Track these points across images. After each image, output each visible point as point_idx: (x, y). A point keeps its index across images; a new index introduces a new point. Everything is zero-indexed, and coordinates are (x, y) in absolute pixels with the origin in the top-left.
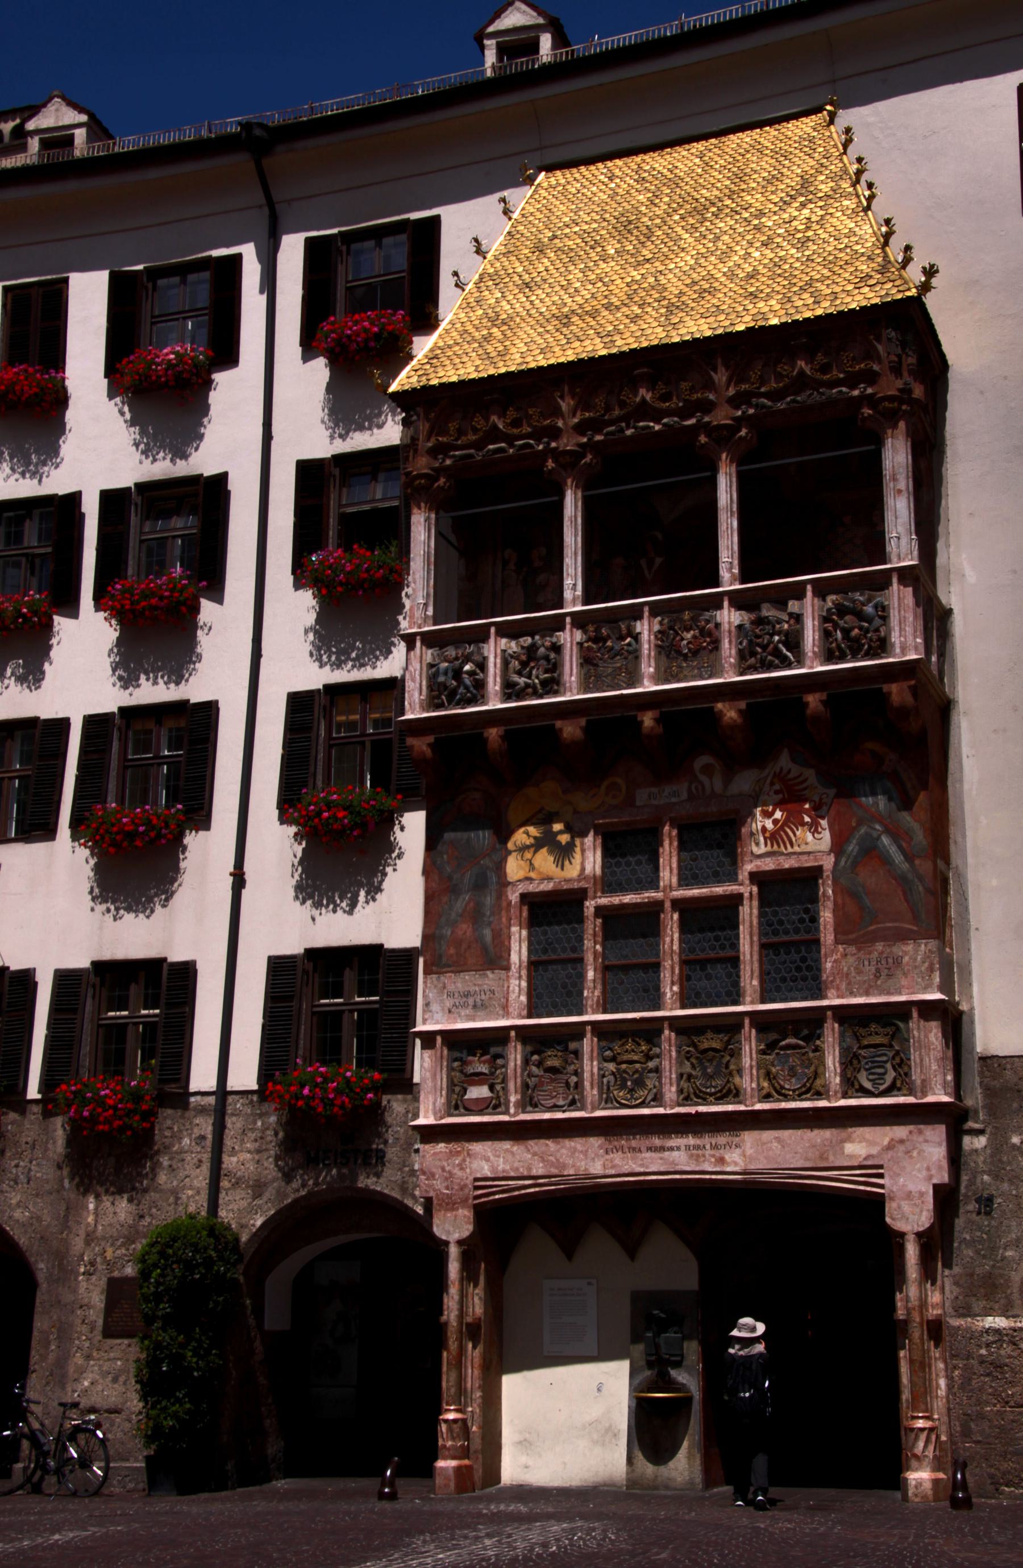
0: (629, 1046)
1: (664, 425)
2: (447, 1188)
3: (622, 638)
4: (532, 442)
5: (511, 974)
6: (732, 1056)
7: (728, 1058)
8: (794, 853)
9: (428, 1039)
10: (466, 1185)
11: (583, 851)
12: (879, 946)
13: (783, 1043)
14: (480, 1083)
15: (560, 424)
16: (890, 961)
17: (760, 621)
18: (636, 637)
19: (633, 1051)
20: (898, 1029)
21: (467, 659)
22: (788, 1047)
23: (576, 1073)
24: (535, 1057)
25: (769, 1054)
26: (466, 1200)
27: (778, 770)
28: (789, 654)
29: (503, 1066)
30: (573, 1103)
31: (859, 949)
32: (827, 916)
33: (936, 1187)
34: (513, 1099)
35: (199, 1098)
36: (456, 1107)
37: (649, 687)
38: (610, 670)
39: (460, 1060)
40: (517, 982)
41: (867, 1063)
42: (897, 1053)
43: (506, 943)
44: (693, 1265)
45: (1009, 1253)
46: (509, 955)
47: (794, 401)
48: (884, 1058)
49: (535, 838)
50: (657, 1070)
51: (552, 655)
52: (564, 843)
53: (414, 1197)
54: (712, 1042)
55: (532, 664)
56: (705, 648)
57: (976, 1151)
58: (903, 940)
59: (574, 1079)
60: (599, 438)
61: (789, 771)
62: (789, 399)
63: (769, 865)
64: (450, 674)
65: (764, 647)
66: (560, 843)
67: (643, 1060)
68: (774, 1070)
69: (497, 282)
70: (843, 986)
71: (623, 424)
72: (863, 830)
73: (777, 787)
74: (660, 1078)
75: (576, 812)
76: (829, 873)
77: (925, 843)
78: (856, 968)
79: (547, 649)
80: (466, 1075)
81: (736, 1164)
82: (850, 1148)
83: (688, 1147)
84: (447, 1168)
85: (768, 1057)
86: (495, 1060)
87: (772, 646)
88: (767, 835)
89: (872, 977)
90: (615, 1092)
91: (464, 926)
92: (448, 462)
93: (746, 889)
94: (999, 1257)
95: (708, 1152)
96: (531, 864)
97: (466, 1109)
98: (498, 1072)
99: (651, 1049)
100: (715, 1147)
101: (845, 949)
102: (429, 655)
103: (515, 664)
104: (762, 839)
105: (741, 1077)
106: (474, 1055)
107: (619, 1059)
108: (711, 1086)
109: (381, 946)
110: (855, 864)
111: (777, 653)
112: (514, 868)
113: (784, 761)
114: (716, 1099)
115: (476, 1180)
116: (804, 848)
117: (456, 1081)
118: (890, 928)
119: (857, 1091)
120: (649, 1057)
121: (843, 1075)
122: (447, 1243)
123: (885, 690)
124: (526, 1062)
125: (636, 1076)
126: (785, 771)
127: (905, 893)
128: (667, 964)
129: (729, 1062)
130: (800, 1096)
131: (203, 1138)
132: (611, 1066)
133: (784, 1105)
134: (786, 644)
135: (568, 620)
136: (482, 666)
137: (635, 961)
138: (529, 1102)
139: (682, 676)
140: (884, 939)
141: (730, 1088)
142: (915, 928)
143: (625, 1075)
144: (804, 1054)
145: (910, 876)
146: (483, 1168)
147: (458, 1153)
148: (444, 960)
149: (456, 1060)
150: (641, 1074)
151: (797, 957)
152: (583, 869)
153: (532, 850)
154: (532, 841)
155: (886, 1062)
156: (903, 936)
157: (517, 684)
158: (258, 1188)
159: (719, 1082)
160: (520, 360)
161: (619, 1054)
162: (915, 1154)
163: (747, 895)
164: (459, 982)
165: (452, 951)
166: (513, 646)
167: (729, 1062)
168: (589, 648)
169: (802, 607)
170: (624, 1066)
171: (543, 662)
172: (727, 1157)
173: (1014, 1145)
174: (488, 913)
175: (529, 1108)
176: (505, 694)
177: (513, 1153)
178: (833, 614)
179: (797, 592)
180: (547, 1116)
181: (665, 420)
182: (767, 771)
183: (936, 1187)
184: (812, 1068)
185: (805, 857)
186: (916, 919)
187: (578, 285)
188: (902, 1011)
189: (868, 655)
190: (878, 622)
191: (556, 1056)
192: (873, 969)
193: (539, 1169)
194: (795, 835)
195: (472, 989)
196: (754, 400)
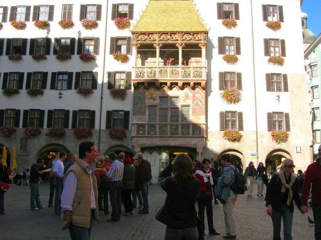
12: (198, 116)
14: (142, 131)
15: (157, 39)
23: (155, 130)
34: (146, 133)
35: (96, 130)
60: (163, 42)
72: (196, 100)
82: (193, 142)
100: (175, 141)
103: (149, 74)
104: (182, 100)
112: (147, 101)
113: (187, 90)
121: (192, 132)
124: (148, 128)
128: (169, 116)
130: (186, 135)
131: (97, 136)
133: (184, 136)
138: (149, 134)
145: (202, 107)
147: (138, 140)
156: (201, 115)
158: (106, 143)
164: (138, 116)
166: (150, 70)
180: (151, 136)
190: (201, 74)
193: (150, 143)
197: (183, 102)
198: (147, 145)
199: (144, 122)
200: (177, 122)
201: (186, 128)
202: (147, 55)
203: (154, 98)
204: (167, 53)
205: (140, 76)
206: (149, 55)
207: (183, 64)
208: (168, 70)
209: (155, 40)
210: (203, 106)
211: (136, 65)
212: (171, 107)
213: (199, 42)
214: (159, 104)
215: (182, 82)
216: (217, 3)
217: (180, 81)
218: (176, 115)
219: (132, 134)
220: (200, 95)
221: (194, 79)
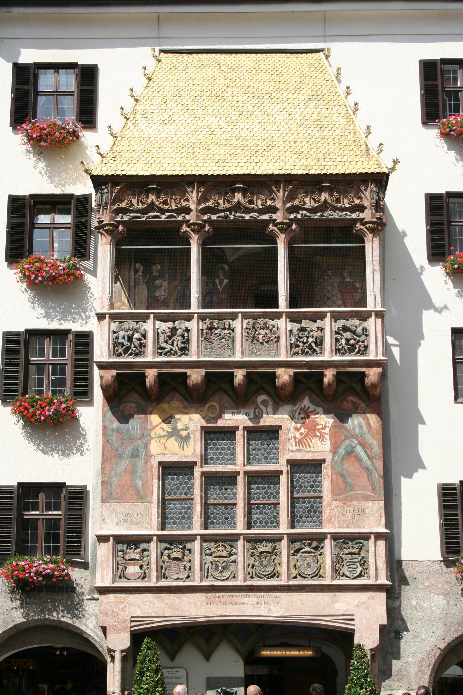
0: (220, 548)
1: (251, 217)
2: (116, 622)
3: (225, 329)
4: (175, 215)
5: (153, 505)
6: (276, 556)
7: (274, 557)
8: (311, 451)
9: (102, 539)
10: (126, 620)
11: (195, 441)
12: (354, 502)
13: (303, 550)
14: (134, 564)
15: (193, 207)
16: (360, 510)
17: (302, 330)
18: (233, 330)
19: (223, 551)
20: (363, 545)
21: (137, 331)
22: (306, 552)
23: (190, 561)
24: (166, 552)
25: (296, 555)
26: (125, 628)
27: (303, 407)
28: (316, 349)
29: (148, 556)
30: (188, 577)
31: (344, 504)
32: (326, 485)
33: (380, 626)
36: (120, 577)
37: (238, 357)
38: (219, 346)
39: (123, 551)
40: (156, 510)
41: (347, 563)
42: (363, 558)
43: (150, 488)
44: (241, 663)
45: (410, 659)
46: (152, 495)
47: (322, 215)
48: (357, 560)
49: (167, 432)
50: (235, 562)
51: (186, 335)
52: (184, 436)
53: (86, 625)
54: (265, 547)
55: (174, 338)
56: (272, 340)
57: (395, 608)
58: (367, 500)
59: (188, 565)
60: (214, 217)
61: (309, 408)
62: (319, 214)
63: (298, 456)
64: (126, 338)
65: (304, 343)
66: (181, 436)
67: (228, 556)
68: (298, 564)
69: (145, 116)
70: (336, 523)
71: (228, 213)
72: (347, 442)
73: (302, 415)
74: (237, 566)
75: (190, 419)
76: (329, 463)
77: (379, 451)
78: (342, 513)
79: (183, 331)
80: (126, 560)
81: (278, 611)
83: (252, 603)
84: (115, 611)
85: (295, 557)
86: (143, 553)
87: (308, 343)
88: (297, 440)
89: (351, 518)
90: (213, 573)
91: (125, 478)
92: (126, 218)
93: (285, 468)
94: (405, 662)
95: (263, 606)
96: (165, 446)
97: (126, 578)
98: (145, 559)
99: (232, 550)
101: (337, 503)
102: (114, 326)
105: (281, 567)
106: (131, 549)
107: (215, 555)
108: (265, 571)
109: (64, 483)
110: (343, 459)
111: (310, 347)
113: (306, 402)
114: (268, 578)
115: (132, 617)
116: (316, 449)
117: (120, 563)
118: (360, 494)
119: (342, 576)
120: (231, 555)
122: (114, 651)
123: (366, 373)
124: (162, 554)
125: (224, 564)
126: (307, 407)
127: (368, 477)
129: (275, 558)
132: (210, 559)
134: (316, 343)
135: (196, 316)
136: (144, 336)
137: (221, 502)
139: (258, 354)
140: (357, 499)
141: (275, 573)
142: (373, 495)
143: (218, 563)
144: (315, 556)
145: (371, 468)
146: (136, 611)
148: (113, 496)
149: (120, 551)
150: (227, 563)
151: (309, 505)
152: (195, 451)
153: (166, 438)
154: (166, 433)
155: (357, 562)
156: (367, 498)
157: (164, 349)
159: (269, 569)
160: (169, 168)
161: (214, 552)
162: (370, 609)
163: (285, 472)
165: (119, 491)
167: (275, 558)
168: (207, 333)
169: (324, 325)
170: (217, 559)
171: (180, 338)
172: (273, 608)
173: (412, 606)
174: (140, 471)
175: (163, 579)
176: (158, 353)
177: (154, 603)
178: (340, 330)
179: (322, 316)
180: (175, 584)
181: (251, 214)
182: (297, 407)
183: (380, 626)
184: (319, 563)
185: (317, 453)
186: (373, 489)
187: (194, 127)
188: (366, 537)
189: (358, 353)
190: (363, 338)
191: (179, 551)
192: (351, 514)
194: (311, 441)
195: (131, 512)
196: (300, 211)
197: (294, 448)
198: (157, 623)
199: (146, 529)
200: (275, 527)
201: (309, 552)
202: (154, 267)
203: (184, 433)
204: (231, 258)
205: (128, 348)
206: (159, 267)
207: (293, 303)
208: (237, 324)
209: (187, 210)
210: (372, 463)
211: (112, 306)
212: (249, 468)
213: (354, 216)
214: (205, 461)
215: (291, 371)
216: (421, 62)
217: (283, 369)
218: (269, 501)
219: (98, 575)
220: (361, 420)
221: (338, 358)
